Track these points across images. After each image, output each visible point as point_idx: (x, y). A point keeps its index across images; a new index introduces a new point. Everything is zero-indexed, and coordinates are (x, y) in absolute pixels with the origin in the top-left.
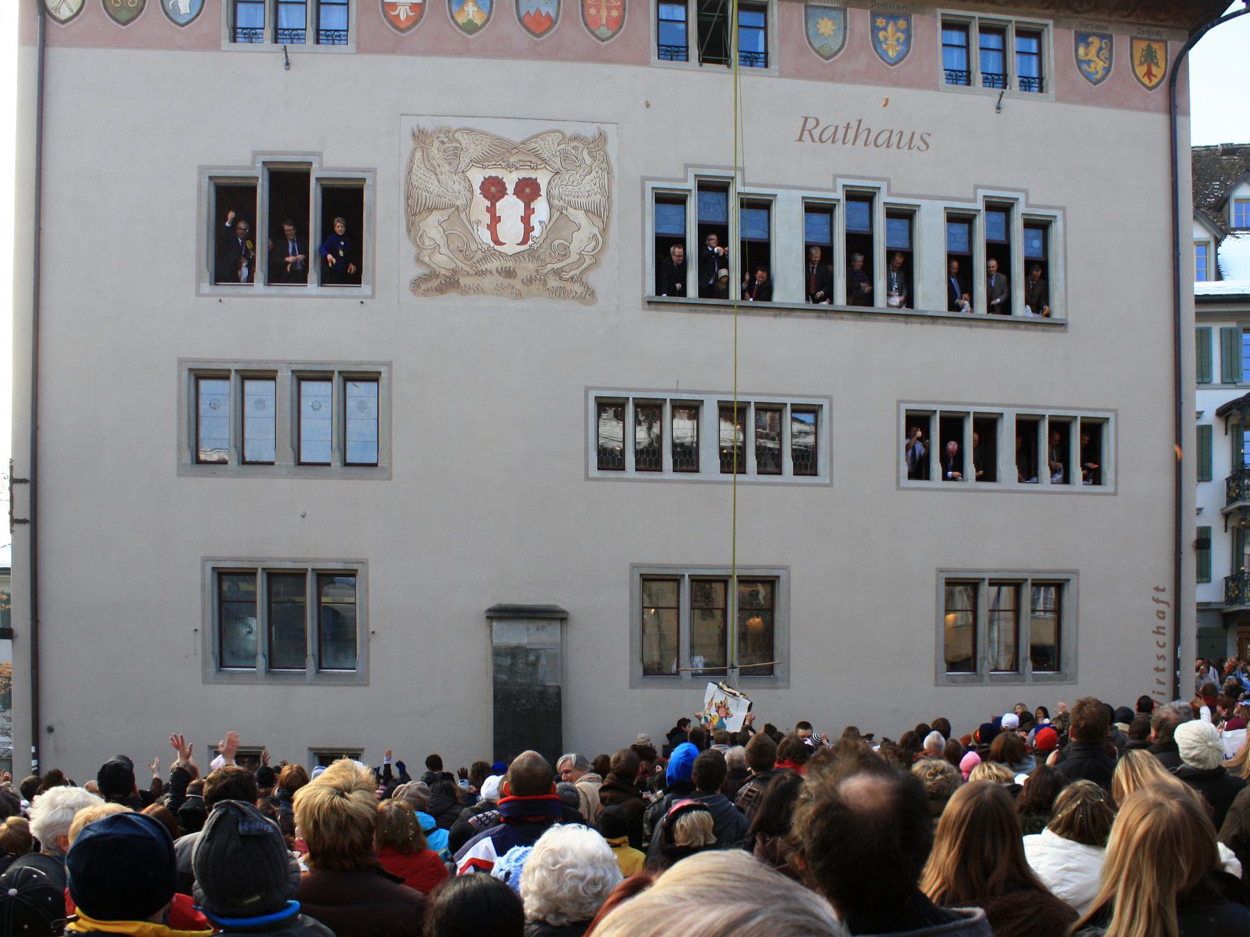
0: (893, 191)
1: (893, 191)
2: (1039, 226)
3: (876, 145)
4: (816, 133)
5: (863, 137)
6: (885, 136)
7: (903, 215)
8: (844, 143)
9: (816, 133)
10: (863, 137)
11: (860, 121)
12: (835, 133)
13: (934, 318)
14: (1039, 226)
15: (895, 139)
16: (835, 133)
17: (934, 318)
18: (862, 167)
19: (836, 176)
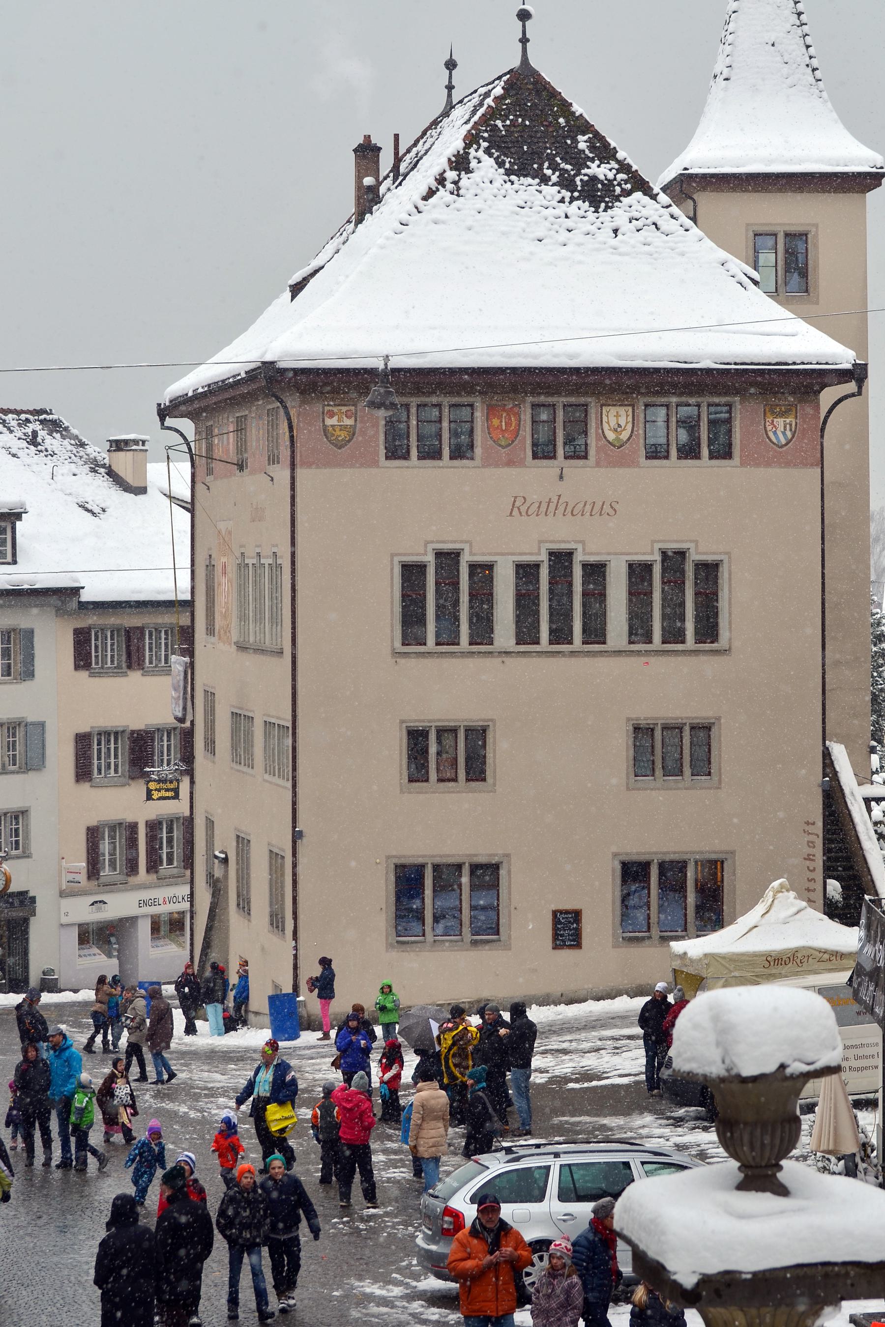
0: (587, 550)
1: (587, 550)
2: (709, 571)
3: (573, 515)
4: (523, 509)
5: (561, 508)
6: (581, 505)
7: (596, 572)
8: (546, 514)
9: (523, 509)
10: (561, 508)
11: (560, 496)
12: (539, 507)
13: (618, 653)
14: (709, 571)
15: (588, 508)
16: (539, 507)
17: (618, 653)
18: (560, 533)
19: (540, 542)
